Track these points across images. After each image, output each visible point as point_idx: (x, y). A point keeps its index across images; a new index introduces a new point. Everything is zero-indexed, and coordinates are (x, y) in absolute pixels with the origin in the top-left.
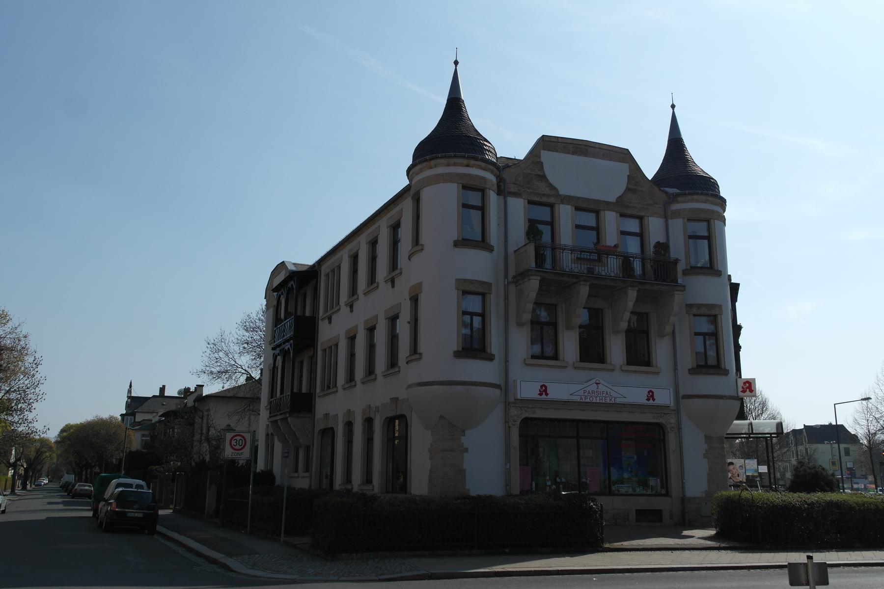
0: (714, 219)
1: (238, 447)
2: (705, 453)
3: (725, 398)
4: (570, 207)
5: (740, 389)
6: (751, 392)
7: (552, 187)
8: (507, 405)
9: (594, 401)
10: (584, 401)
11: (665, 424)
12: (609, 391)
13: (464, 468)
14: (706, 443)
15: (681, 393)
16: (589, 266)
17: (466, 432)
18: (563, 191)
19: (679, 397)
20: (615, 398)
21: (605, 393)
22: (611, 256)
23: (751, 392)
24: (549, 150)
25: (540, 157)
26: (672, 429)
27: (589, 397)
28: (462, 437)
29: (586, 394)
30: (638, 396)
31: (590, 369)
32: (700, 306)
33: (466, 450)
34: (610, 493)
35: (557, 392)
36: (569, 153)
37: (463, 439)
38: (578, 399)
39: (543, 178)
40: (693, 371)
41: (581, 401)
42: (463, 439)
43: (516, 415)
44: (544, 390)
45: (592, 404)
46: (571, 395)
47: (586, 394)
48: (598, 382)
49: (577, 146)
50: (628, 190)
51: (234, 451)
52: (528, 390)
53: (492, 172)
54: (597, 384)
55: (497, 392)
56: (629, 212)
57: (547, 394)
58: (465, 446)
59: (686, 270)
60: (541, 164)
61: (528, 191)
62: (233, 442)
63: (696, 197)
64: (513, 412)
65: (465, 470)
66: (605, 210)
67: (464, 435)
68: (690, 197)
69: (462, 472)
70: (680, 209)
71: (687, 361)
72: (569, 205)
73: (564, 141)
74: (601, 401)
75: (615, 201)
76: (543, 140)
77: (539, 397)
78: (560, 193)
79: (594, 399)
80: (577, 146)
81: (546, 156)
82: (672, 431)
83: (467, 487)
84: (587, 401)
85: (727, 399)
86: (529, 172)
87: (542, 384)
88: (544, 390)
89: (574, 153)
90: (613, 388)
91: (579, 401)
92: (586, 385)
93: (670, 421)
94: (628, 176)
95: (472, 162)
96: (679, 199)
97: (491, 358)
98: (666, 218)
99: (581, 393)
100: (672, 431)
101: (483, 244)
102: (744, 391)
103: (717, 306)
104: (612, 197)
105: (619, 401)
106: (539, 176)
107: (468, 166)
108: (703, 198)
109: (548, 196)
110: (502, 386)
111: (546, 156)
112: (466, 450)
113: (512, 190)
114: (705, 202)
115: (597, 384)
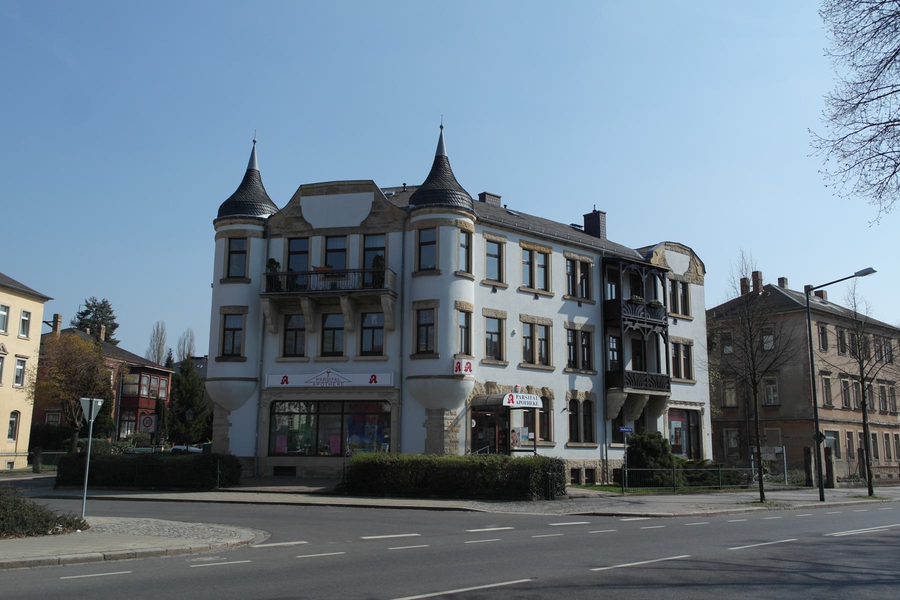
0: (439, 226)
1: (147, 425)
2: (424, 422)
4: (320, 237)
5: (455, 369)
8: (261, 391)
12: (337, 377)
14: (426, 415)
15: (405, 376)
17: (231, 412)
18: (315, 226)
19: (401, 377)
20: (342, 382)
24: (306, 195)
25: (299, 203)
26: (394, 405)
28: (229, 416)
29: (318, 381)
30: (362, 380)
31: (328, 361)
32: (419, 302)
33: (231, 425)
34: (317, 455)
35: (295, 381)
36: (323, 195)
38: (311, 385)
39: (301, 218)
40: (413, 357)
43: (268, 398)
44: (285, 380)
45: (322, 388)
47: (318, 381)
49: (331, 187)
50: (372, 213)
51: (145, 428)
52: (273, 380)
53: (254, 224)
54: (328, 373)
55: (251, 384)
56: (371, 232)
57: (287, 383)
58: (230, 422)
59: (415, 272)
60: (299, 208)
61: (288, 231)
62: (145, 422)
63: (422, 210)
64: (265, 396)
65: (229, 439)
68: (417, 211)
69: (227, 440)
71: (410, 348)
73: (318, 185)
76: (301, 189)
79: (325, 384)
81: (304, 201)
83: (230, 450)
84: (318, 386)
86: (289, 216)
87: (284, 375)
88: (285, 380)
89: (326, 194)
90: (341, 375)
94: (373, 202)
95: (234, 221)
96: (413, 213)
97: (243, 360)
98: (404, 231)
99: (315, 380)
101: (242, 279)
102: (466, 370)
103: (433, 300)
104: (357, 223)
105: (344, 385)
107: (231, 224)
108: (428, 209)
109: (302, 232)
110: (258, 379)
111: (304, 201)
113: (276, 233)
114: (431, 212)
115: (328, 373)
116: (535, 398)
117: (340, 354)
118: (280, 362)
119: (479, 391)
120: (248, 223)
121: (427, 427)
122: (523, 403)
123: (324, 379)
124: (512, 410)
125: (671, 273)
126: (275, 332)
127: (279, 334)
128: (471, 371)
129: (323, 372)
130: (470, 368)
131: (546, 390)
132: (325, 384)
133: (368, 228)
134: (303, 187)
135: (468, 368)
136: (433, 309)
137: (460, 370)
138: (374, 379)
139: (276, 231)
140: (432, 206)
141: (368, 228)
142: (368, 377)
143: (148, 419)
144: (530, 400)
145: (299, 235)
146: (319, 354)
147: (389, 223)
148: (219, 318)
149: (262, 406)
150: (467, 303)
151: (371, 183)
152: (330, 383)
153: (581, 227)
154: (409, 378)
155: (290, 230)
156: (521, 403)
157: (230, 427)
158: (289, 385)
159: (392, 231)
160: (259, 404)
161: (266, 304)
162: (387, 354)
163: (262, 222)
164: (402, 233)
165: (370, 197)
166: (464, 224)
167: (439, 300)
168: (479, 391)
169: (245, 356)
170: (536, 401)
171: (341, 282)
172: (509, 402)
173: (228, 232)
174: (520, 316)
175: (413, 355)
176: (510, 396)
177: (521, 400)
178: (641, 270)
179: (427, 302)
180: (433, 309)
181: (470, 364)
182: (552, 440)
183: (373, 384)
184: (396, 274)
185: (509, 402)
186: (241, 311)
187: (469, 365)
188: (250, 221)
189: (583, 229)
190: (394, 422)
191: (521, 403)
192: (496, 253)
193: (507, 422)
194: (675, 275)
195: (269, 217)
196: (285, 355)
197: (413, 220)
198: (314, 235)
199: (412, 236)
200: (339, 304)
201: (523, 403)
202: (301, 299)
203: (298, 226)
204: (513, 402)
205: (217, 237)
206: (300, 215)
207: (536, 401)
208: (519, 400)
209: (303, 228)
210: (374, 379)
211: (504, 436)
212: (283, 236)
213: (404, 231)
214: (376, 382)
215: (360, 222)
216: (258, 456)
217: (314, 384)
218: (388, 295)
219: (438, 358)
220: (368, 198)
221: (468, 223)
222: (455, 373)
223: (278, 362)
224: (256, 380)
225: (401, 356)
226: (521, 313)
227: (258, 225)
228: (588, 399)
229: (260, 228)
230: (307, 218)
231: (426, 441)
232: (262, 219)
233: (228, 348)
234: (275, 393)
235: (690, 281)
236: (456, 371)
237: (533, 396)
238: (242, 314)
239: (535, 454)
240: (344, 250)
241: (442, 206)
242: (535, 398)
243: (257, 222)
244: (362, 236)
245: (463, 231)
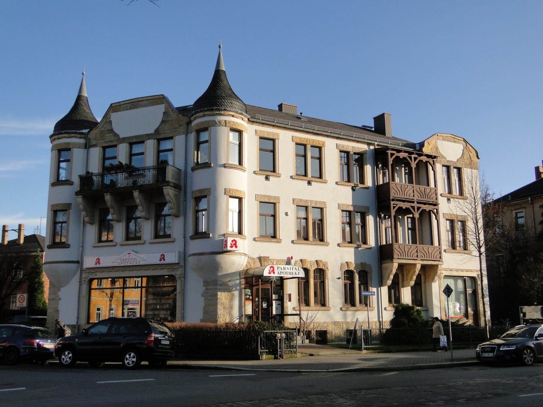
0: (211, 127)
1: (22, 301)
3: (205, 254)
4: (125, 144)
5: (224, 246)
6: (236, 248)
7: (116, 135)
8: (82, 271)
13: (59, 309)
14: (204, 286)
16: (134, 179)
18: (121, 136)
19: (184, 256)
21: (133, 259)
22: (119, 174)
23: (236, 248)
26: (179, 278)
27: (123, 263)
29: (122, 261)
33: (60, 299)
35: (106, 262)
36: (127, 110)
37: (59, 293)
39: (111, 131)
46: (113, 262)
47: (122, 261)
48: (129, 252)
50: (163, 121)
51: (20, 304)
52: (89, 262)
53: (76, 137)
54: (129, 254)
56: (162, 137)
60: (110, 122)
62: (20, 299)
63: (197, 115)
64: (84, 275)
66: (146, 140)
72: (125, 143)
75: (154, 132)
76: (112, 107)
77: (95, 265)
78: (120, 138)
81: (114, 116)
85: (206, 255)
92: (122, 255)
93: (178, 273)
94: (164, 112)
98: (187, 133)
99: (119, 261)
101: (68, 182)
104: (152, 131)
105: (142, 263)
106: (108, 130)
111: (114, 116)
113: (94, 143)
114: (204, 116)
115: (129, 254)
116: (297, 269)
117: (139, 238)
118: (96, 247)
119: (252, 265)
120: (72, 137)
121: (204, 297)
122: (284, 273)
123: (126, 259)
124: (285, 281)
125: (444, 160)
126: (92, 223)
127: (95, 225)
128: (236, 247)
129: (124, 254)
131: (320, 262)
134: (113, 105)
135: (234, 245)
137: (227, 247)
138: (163, 257)
139: (94, 142)
142: (158, 256)
143: (22, 297)
144: (291, 271)
145: (110, 144)
146: (124, 239)
147: (176, 128)
148: (51, 213)
150: (237, 190)
151: (162, 97)
153: (372, 128)
154: (190, 256)
155: (104, 141)
156: (282, 274)
158: (101, 265)
159: (178, 134)
160: (80, 282)
161: (80, 199)
163: (83, 136)
165: (160, 109)
166: (233, 124)
167: (210, 189)
168: (252, 265)
169: (69, 243)
171: (139, 179)
172: (270, 273)
173: (59, 144)
174: (293, 200)
176: (270, 267)
177: (283, 271)
178: (410, 158)
179: (201, 191)
181: (236, 241)
182: (327, 305)
184: (180, 170)
185: (270, 273)
186: (65, 208)
187: (234, 242)
188: (73, 135)
189: (373, 129)
190: (179, 293)
191: (282, 274)
192: (318, 156)
193: (282, 291)
194: (448, 161)
195: (89, 132)
197: (194, 123)
198: (121, 143)
199: (192, 137)
200: (132, 197)
201: (284, 273)
202: (105, 194)
203: (109, 137)
204: (274, 273)
205: (52, 149)
206: (109, 128)
208: (280, 271)
209: (113, 139)
210: (163, 257)
212: (99, 146)
213: (187, 133)
215: (155, 129)
216: (79, 324)
217: (119, 264)
218: (169, 187)
219: (209, 237)
220: (160, 109)
221: (237, 123)
224: (78, 262)
226: (294, 198)
227: (80, 138)
228: (363, 269)
229: (82, 141)
230: (116, 130)
231: (204, 308)
232: (82, 133)
234: (92, 273)
235: (464, 166)
237: (291, 266)
238: (66, 210)
239: (301, 318)
240: (142, 154)
242: (297, 269)
243: (78, 136)
244: (156, 140)
245: (233, 130)
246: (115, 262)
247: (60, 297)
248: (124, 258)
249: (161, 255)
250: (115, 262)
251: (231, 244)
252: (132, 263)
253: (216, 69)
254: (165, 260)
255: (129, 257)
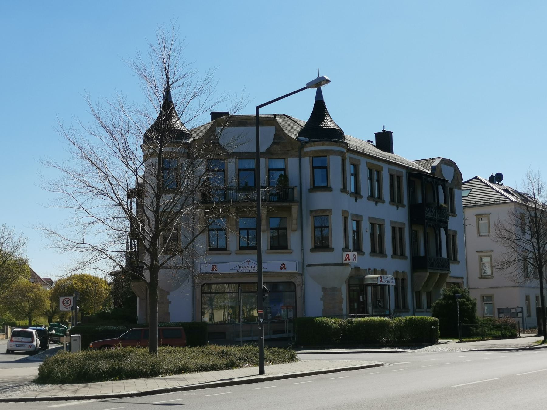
1: (67, 305)
5: (344, 259)
9: (246, 272)
10: (239, 272)
11: (294, 282)
13: (169, 312)
14: (322, 292)
17: (170, 293)
19: (303, 265)
26: (299, 285)
32: (316, 211)
33: (170, 302)
35: (222, 269)
40: (312, 250)
41: (238, 272)
42: (168, 297)
50: (274, 143)
51: (65, 307)
52: (205, 268)
62: (64, 302)
67: (169, 294)
68: (312, 143)
70: (308, 151)
71: (309, 243)
74: (250, 272)
75: (265, 152)
79: (246, 271)
80: (240, 121)
82: (299, 286)
84: (241, 272)
91: (236, 272)
92: (240, 263)
93: (297, 280)
94: (274, 134)
96: (307, 145)
98: (300, 157)
99: (238, 268)
100: (299, 286)
103: (328, 210)
112: (170, 302)
130: (348, 258)
132: (246, 271)
133: (272, 154)
136: (328, 216)
138: (283, 266)
140: (324, 141)
141: (272, 154)
143: (67, 300)
147: (288, 150)
149: (195, 288)
152: (250, 270)
157: (169, 304)
159: (292, 156)
162: (291, 248)
164: (298, 158)
170: (392, 280)
175: (312, 249)
179: (323, 211)
180: (328, 216)
183: (283, 270)
190: (299, 298)
196: (210, 249)
197: (306, 149)
199: (306, 162)
207: (392, 280)
210: (283, 266)
211: (363, 305)
213: (300, 157)
214: (285, 269)
222: (345, 262)
223: (236, 254)
225: (303, 249)
233: (214, 243)
234: (206, 278)
236: (346, 260)
241: (331, 141)
246: (235, 268)
247: (169, 301)
248: (244, 265)
249: (282, 265)
250: (235, 268)
251: (345, 258)
252: (252, 270)
253: (315, 100)
254: (286, 269)
255: (248, 265)
